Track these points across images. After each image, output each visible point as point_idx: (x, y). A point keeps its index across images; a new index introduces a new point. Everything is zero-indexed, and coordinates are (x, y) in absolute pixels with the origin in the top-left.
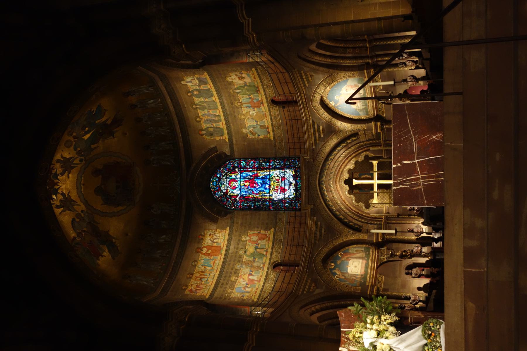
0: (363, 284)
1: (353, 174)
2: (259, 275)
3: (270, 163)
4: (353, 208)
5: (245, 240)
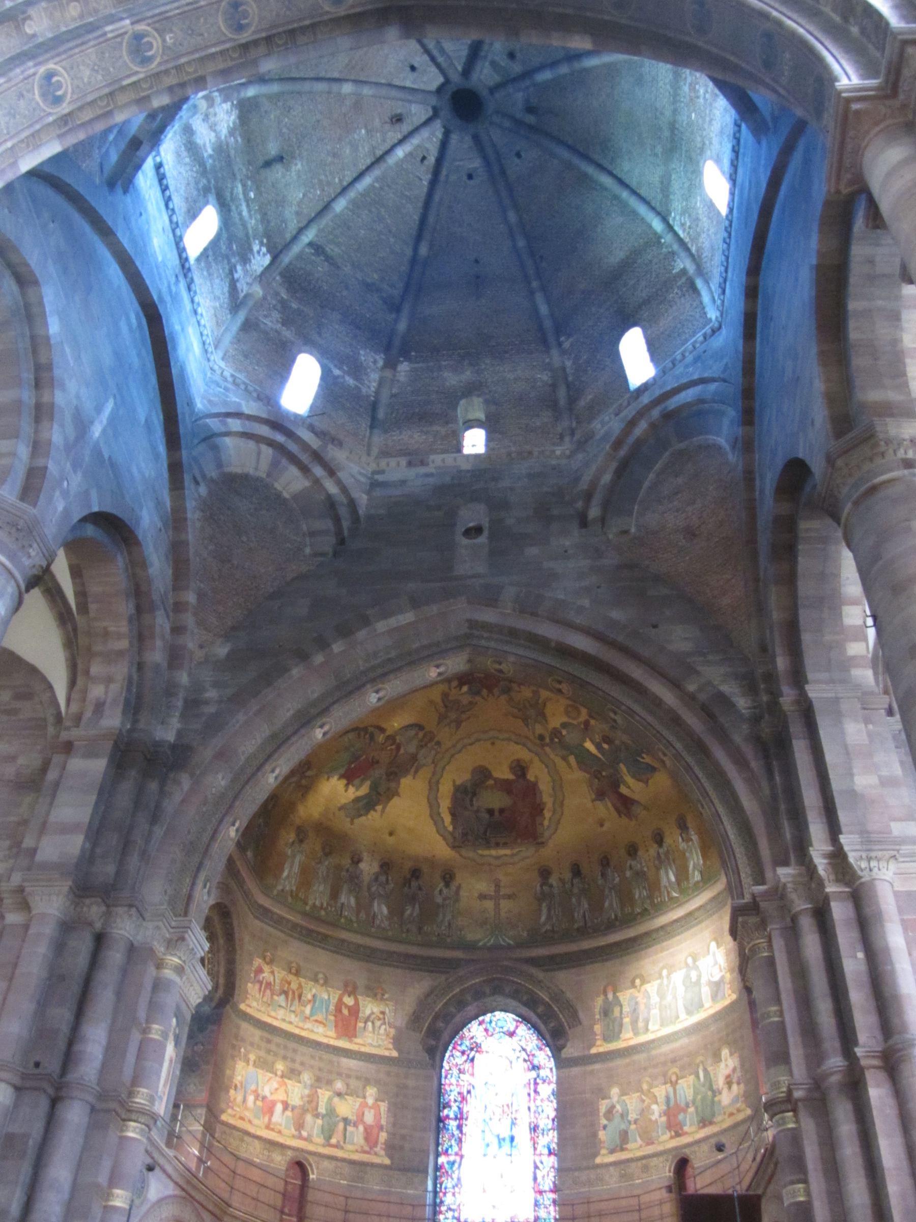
2: (282, 1128)
3: (550, 1153)
5: (367, 1094)
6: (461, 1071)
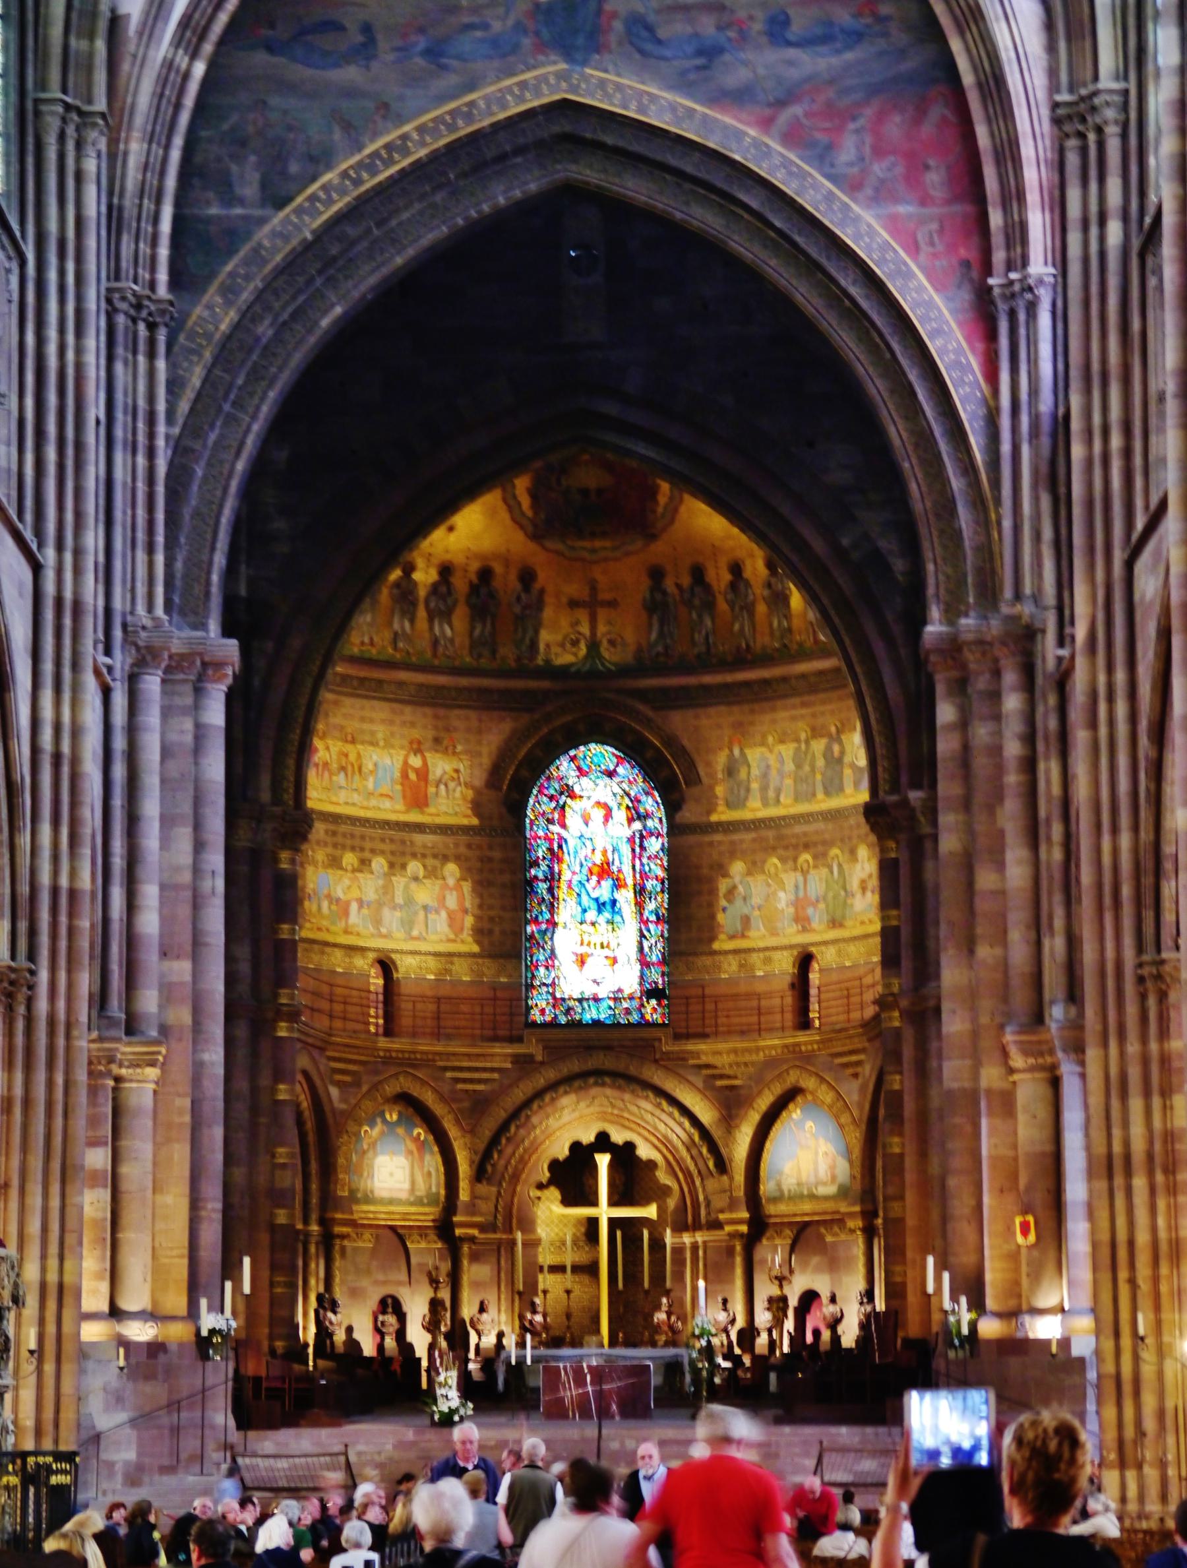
0: (353, 1198)
1: (624, 1156)
2: (361, 929)
3: (657, 923)
4: (534, 1157)
6: (550, 821)
